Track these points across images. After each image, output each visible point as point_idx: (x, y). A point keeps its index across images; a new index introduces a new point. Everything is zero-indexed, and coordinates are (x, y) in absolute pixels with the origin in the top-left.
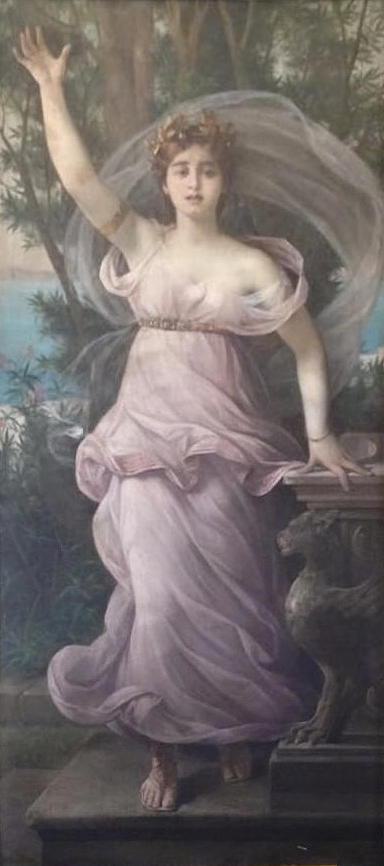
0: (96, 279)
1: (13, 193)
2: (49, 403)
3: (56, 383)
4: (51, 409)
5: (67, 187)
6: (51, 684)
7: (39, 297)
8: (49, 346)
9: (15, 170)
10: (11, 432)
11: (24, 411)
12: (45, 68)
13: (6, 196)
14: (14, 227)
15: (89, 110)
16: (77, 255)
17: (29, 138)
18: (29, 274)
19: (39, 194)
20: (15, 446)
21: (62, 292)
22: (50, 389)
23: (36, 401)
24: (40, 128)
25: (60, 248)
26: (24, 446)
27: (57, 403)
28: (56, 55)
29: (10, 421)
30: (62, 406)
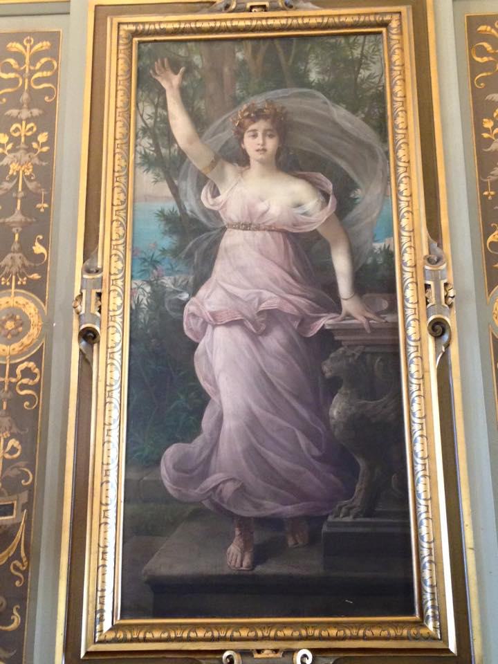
0: (199, 200)
1: (147, 151)
2: (166, 278)
3: (171, 265)
4: (168, 282)
5: (181, 147)
6: (163, 471)
7: (162, 212)
8: (167, 242)
9: (149, 138)
10: (141, 297)
11: (150, 283)
12: (169, 80)
13: (143, 153)
14: (148, 170)
15: (196, 102)
16: (187, 186)
17: (158, 119)
18: (153, 198)
19: (163, 151)
20: (143, 306)
21: (176, 209)
22: (168, 269)
23: (158, 277)
24: (165, 113)
25: (176, 182)
26: (149, 306)
27: (172, 277)
28: (176, 73)
29: (141, 290)
30: (175, 279)
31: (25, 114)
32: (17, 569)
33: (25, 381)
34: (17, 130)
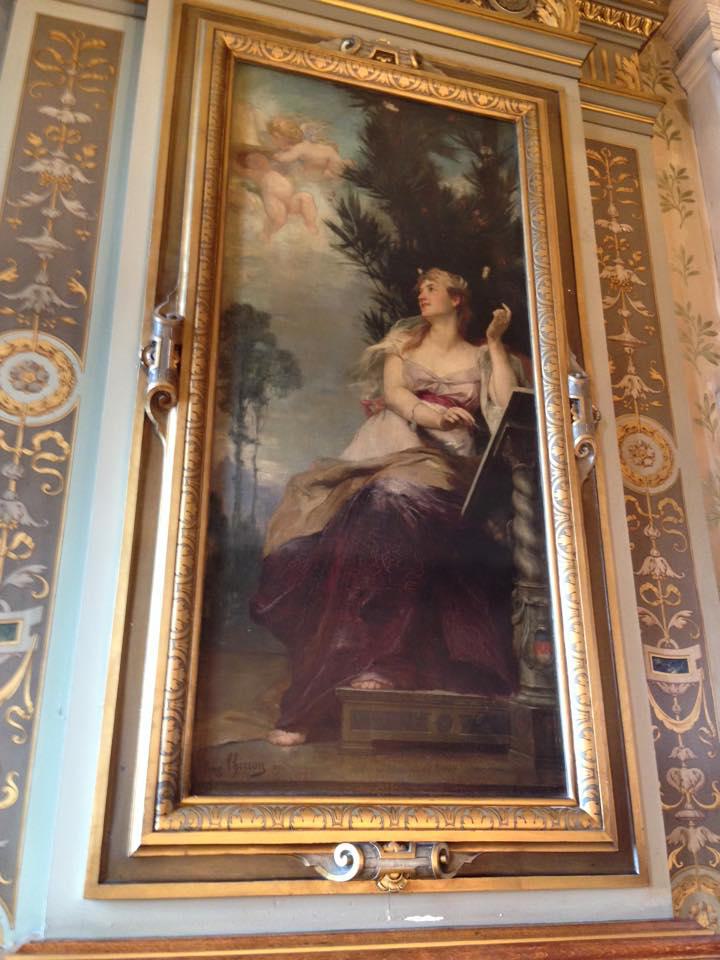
31: (68, 116)
32: (14, 715)
33: (48, 456)
34: (54, 133)
